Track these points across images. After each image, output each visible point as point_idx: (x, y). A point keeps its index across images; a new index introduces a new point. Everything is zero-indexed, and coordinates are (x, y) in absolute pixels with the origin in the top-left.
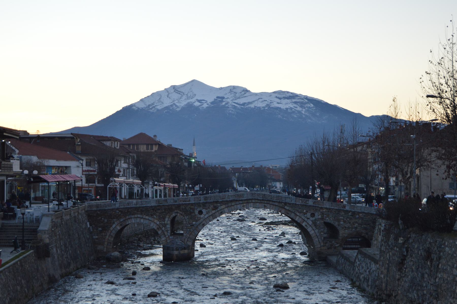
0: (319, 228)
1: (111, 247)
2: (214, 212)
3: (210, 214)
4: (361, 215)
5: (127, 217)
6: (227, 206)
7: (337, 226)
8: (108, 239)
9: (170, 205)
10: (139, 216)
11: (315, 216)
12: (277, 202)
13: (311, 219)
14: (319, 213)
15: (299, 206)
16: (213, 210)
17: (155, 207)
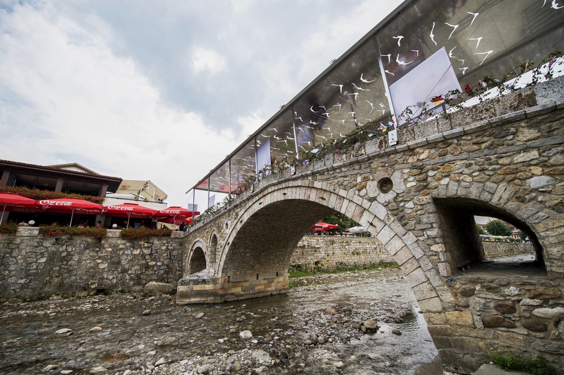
0: (418, 227)
11: (394, 187)
13: (384, 198)
14: (406, 171)
15: (343, 169)
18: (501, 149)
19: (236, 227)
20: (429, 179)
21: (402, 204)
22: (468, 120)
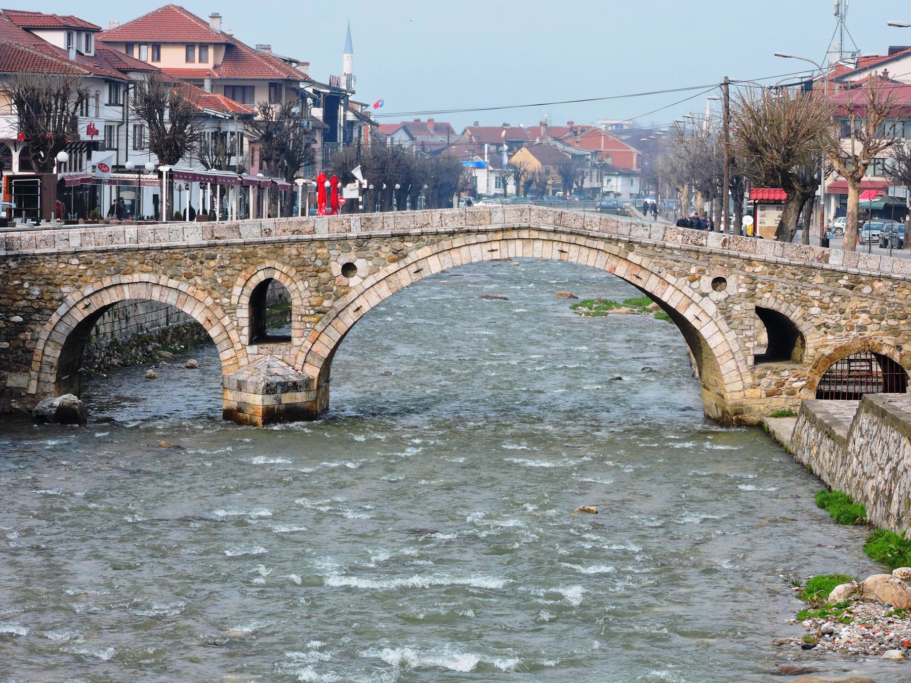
0: (741, 327)
1: (53, 379)
2: (393, 267)
3: (382, 275)
4: (880, 284)
5: (107, 282)
6: (435, 248)
7: (799, 322)
8: (43, 351)
9: (250, 243)
10: (145, 277)
11: (727, 289)
12: (602, 239)
15: (676, 252)
16: (393, 261)
17: (201, 247)
18: (804, 284)
19: (390, 278)
20: (757, 290)
21: (731, 305)
22: (794, 254)
